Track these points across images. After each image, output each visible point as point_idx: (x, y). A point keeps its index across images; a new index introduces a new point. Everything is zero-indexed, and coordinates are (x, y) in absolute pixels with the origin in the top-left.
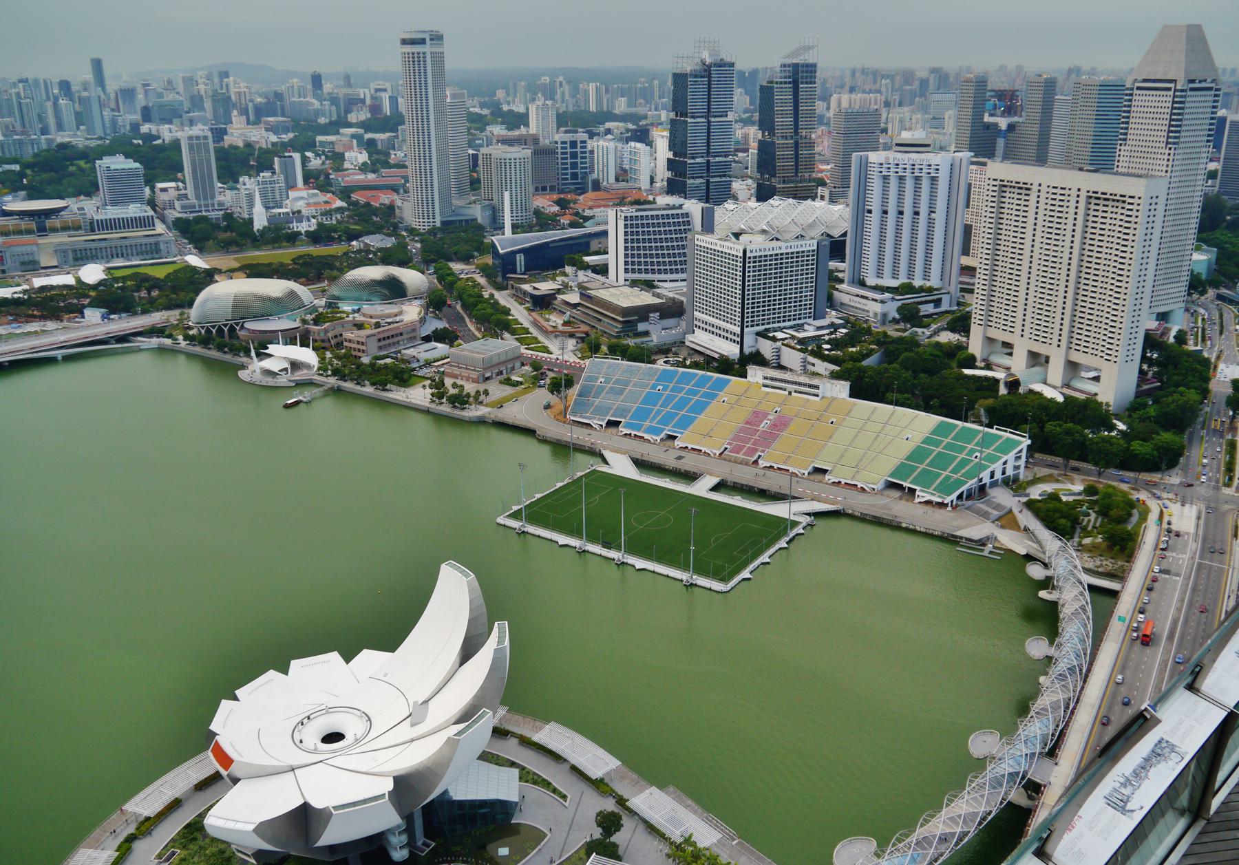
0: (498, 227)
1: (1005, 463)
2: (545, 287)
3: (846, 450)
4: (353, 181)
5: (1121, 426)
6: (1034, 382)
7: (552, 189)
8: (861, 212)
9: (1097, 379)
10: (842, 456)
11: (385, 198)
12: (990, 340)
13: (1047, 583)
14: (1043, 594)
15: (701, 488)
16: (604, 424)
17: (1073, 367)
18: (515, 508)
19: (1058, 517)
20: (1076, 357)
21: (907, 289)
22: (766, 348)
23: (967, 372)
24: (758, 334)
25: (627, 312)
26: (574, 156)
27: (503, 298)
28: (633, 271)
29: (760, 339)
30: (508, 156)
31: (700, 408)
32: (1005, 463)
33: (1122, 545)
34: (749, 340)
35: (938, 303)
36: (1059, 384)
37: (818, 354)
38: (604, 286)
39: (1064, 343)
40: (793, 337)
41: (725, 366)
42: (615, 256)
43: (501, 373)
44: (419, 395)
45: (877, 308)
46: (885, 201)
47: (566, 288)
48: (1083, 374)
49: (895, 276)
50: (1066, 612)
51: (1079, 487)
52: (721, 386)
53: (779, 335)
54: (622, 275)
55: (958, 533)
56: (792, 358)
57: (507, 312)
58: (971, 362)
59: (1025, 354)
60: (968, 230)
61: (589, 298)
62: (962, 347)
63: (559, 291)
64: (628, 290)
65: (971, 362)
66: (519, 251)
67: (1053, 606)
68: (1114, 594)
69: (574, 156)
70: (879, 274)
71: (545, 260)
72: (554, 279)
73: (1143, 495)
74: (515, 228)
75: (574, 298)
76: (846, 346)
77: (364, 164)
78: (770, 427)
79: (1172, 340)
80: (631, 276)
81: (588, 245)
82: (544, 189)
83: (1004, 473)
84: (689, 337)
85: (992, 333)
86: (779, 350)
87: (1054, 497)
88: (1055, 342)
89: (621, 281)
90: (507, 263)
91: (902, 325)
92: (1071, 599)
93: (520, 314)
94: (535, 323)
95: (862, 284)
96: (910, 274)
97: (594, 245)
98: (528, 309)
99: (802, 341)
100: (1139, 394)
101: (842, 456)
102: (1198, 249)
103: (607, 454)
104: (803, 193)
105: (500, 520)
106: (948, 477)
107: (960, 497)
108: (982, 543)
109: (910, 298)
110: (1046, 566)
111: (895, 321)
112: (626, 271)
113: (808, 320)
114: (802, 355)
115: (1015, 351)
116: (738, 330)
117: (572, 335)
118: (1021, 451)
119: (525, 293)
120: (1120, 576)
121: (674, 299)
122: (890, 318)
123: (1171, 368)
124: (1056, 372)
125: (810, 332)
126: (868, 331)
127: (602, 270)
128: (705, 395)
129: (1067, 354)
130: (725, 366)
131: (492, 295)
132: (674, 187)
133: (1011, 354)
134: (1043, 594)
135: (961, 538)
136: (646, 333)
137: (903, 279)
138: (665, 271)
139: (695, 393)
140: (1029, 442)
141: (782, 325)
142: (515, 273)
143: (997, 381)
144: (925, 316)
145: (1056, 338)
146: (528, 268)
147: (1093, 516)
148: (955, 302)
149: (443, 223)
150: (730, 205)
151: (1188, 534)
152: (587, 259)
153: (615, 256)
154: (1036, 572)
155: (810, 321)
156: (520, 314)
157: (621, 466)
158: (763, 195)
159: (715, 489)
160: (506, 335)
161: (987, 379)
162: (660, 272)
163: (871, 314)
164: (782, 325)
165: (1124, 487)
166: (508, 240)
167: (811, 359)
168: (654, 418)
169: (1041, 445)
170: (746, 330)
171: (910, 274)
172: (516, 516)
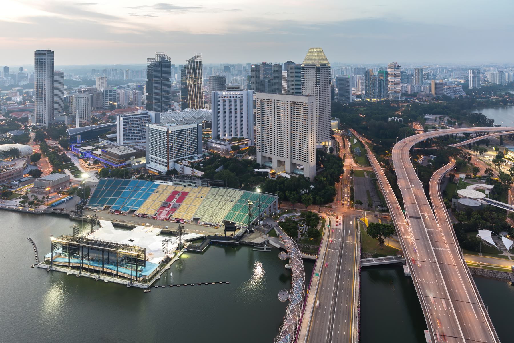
0: (74, 124)
1: (270, 207)
3: (207, 209)
4: (12, 109)
5: (312, 186)
7: (101, 108)
8: (216, 112)
9: (302, 169)
10: (205, 212)
11: (24, 115)
12: (264, 157)
13: (287, 261)
14: (287, 266)
17: (293, 165)
19: (291, 229)
20: (295, 161)
21: (234, 139)
22: (178, 167)
23: (256, 170)
24: (176, 162)
25: (120, 157)
26: (111, 96)
28: (127, 140)
29: (176, 164)
30: (81, 96)
33: (315, 237)
34: (171, 164)
36: (290, 172)
37: (198, 168)
38: (114, 146)
39: (289, 156)
42: (119, 135)
43: (59, 188)
44: (14, 203)
45: (224, 147)
46: (224, 107)
47: (98, 148)
48: (298, 167)
49: (230, 135)
50: (294, 276)
51: (299, 214)
54: (122, 141)
56: (188, 171)
57: (70, 160)
58: (258, 166)
60: (255, 116)
61: (106, 152)
62: (255, 160)
63: (93, 150)
64: (123, 147)
65: (258, 166)
66: (78, 134)
67: (290, 271)
68: (314, 262)
69: (111, 96)
70: (224, 135)
71: (91, 137)
73: (323, 215)
74: (80, 125)
75: (99, 152)
76: (209, 164)
77: (20, 101)
78: (177, 201)
79: (328, 151)
80: (125, 141)
81: (109, 130)
82: (97, 108)
84: (148, 165)
85: (265, 155)
86: (183, 168)
87: (288, 220)
88: (286, 156)
89: (122, 144)
90: (73, 139)
92: (296, 268)
95: (218, 138)
96: (236, 135)
97: (113, 129)
99: (191, 163)
100: (318, 174)
101: (205, 212)
102: (332, 119)
104: (197, 106)
108: (262, 244)
109: (235, 144)
110: (287, 252)
112: (124, 140)
113: (195, 155)
114: (192, 169)
115: (273, 160)
116: (166, 161)
118: (276, 202)
120: (316, 251)
121: (142, 150)
123: (329, 162)
124: (288, 167)
125: (196, 160)
126: (219, 156)
127: (114, 140)
128: (149, 190)
129: (291, 161)
131: (64, 153)
132: (149, 107)
133: (272, 162)
134: (287, 266)
135: (254, 243)
136: (130, 165)
138: (140, 139)
141: (185, 157)
145: (286, 155)
147: (305, 226)
148: (253, 143)
149: (49, 124)
150: (169, 112)
151: (340, 229)
152: (108, 136)
153: (119, 135)
154: (282, 256)
155: (196, 155)
158: (184, 107)
160: (67, 171)
161: (264, 172)
162: (138, 139)
164: (185, 157)
165: (316, 212)
166: (77, 130)
167: (195, 170)
169: (283, 199)
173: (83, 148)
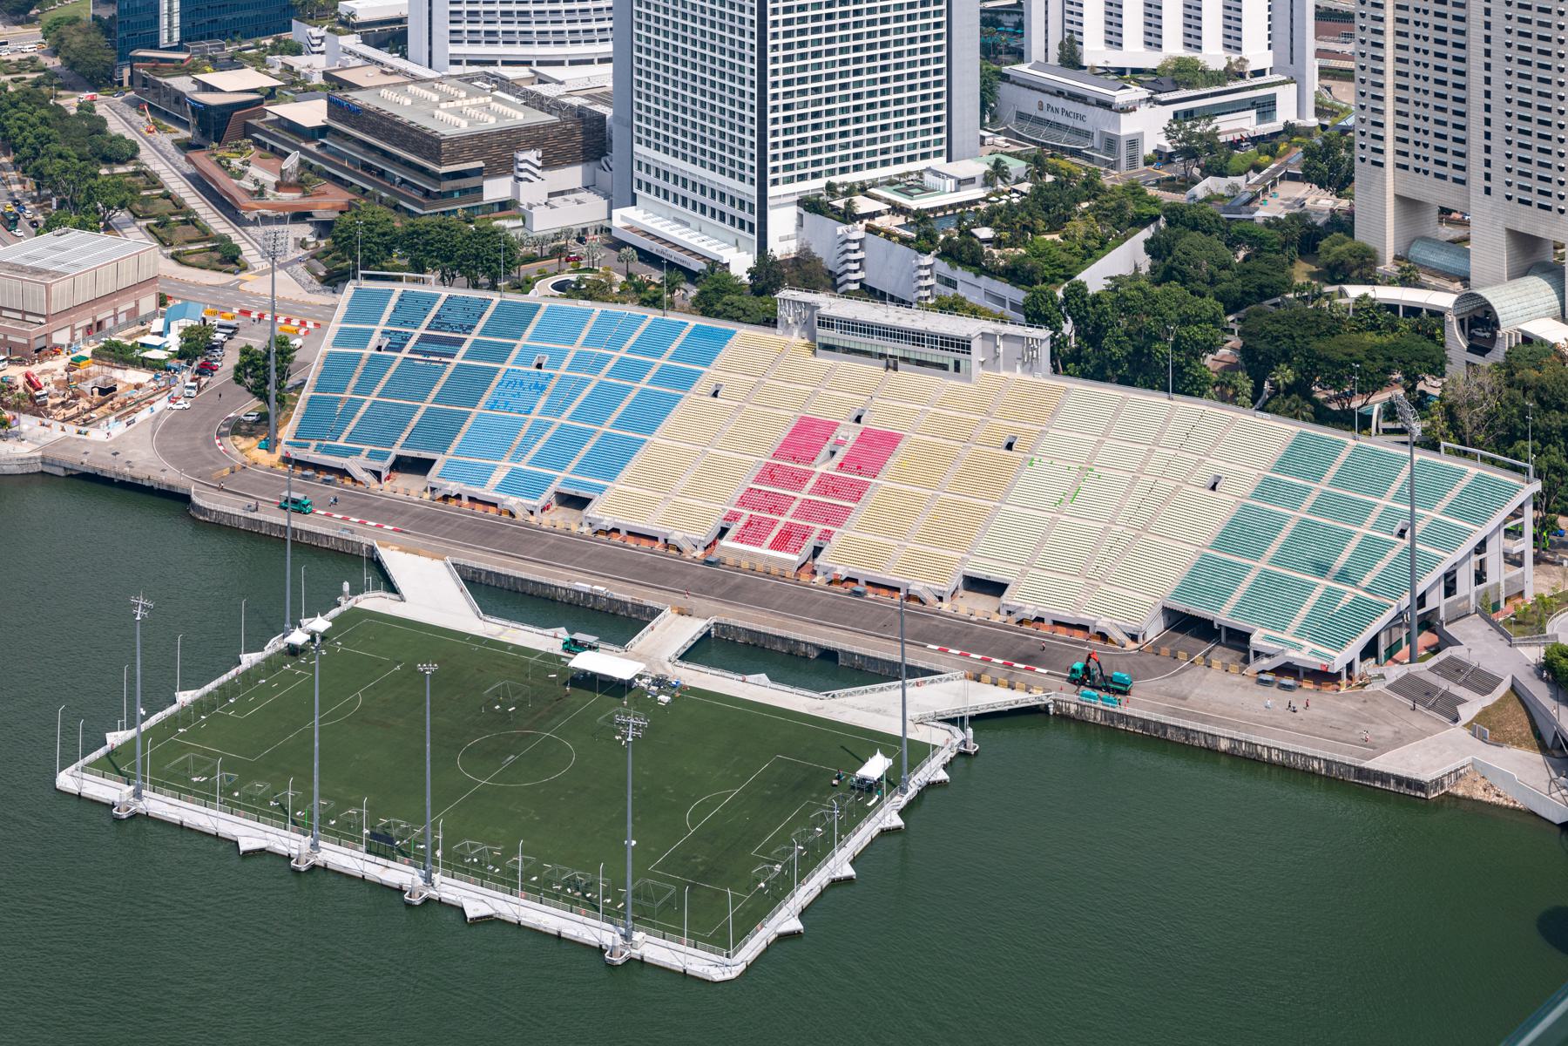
1: (1481, 547)
2: (234, 84)
6: (1532, 317)
15: (655, 654)
16: (384, 466)
18: (115, 738)
21: (1183, 74)
27: (118, 116)
31: (649, 414)
32: (1481, 547)
35: (1265, 108)
37: (963, 254)
40: (897, 209)
41: (715, 295)
52: (706, 348)
53: (863, 205)
55: (1377, 764)
57: (124, 152)
58: (1362, 266)
59: (1502, 241)
62: (1342, 224)
63: (271, 94)
65: (1362, 266)
72: (260, 63)
83: (1480, 577)
91: (1177, 169)
93: (161, 157)
94: (200, 182)
96: (1193, 37)
98: (185, 146)
103: (393, 559)
105: (66, 780)
106: (1331, 596)
107: (1370, 650)
111: (1161, 158)
116: (753, 191)
117: (300, 217)
119: (179, 98)
122: (1148, 150)
128: (664, 376)
130: (715, 295)
137: (1173, 46)
139: (636, 371)
140: (1537, 486)
141: (866, 175)
142: (155, 47)
143: (1437, 314)
144: (1235, 145)
146: (190, 34)
155: (939, 163)
156: (161, 157)
157: (427, 591)
159: (696, 653)
163: (1096, 142)
164: (866, 175)
168: (525, 447)
170: (772, 191)
171: (1193, 37)
172: (113, 765)
173: (211, 78)
